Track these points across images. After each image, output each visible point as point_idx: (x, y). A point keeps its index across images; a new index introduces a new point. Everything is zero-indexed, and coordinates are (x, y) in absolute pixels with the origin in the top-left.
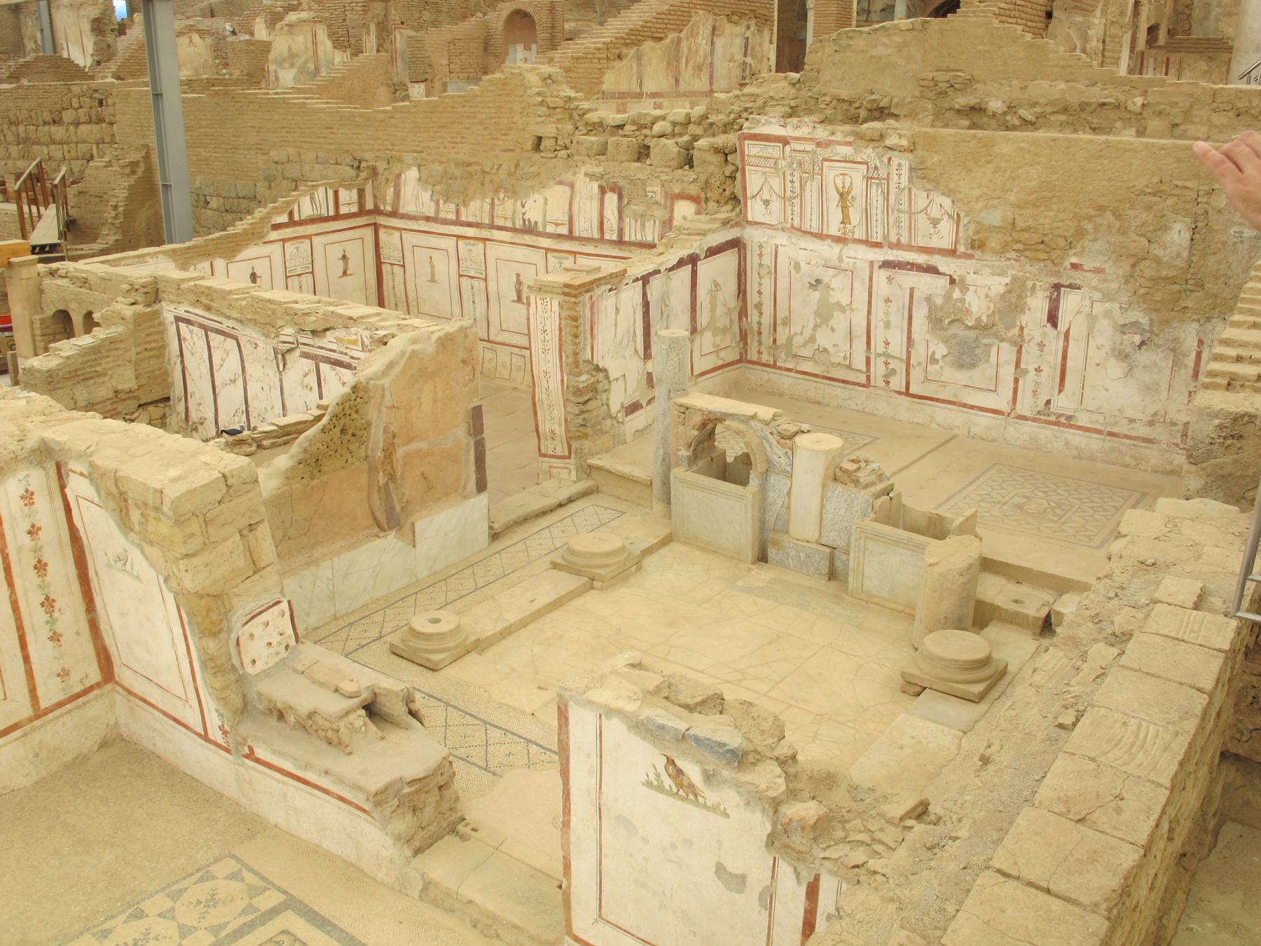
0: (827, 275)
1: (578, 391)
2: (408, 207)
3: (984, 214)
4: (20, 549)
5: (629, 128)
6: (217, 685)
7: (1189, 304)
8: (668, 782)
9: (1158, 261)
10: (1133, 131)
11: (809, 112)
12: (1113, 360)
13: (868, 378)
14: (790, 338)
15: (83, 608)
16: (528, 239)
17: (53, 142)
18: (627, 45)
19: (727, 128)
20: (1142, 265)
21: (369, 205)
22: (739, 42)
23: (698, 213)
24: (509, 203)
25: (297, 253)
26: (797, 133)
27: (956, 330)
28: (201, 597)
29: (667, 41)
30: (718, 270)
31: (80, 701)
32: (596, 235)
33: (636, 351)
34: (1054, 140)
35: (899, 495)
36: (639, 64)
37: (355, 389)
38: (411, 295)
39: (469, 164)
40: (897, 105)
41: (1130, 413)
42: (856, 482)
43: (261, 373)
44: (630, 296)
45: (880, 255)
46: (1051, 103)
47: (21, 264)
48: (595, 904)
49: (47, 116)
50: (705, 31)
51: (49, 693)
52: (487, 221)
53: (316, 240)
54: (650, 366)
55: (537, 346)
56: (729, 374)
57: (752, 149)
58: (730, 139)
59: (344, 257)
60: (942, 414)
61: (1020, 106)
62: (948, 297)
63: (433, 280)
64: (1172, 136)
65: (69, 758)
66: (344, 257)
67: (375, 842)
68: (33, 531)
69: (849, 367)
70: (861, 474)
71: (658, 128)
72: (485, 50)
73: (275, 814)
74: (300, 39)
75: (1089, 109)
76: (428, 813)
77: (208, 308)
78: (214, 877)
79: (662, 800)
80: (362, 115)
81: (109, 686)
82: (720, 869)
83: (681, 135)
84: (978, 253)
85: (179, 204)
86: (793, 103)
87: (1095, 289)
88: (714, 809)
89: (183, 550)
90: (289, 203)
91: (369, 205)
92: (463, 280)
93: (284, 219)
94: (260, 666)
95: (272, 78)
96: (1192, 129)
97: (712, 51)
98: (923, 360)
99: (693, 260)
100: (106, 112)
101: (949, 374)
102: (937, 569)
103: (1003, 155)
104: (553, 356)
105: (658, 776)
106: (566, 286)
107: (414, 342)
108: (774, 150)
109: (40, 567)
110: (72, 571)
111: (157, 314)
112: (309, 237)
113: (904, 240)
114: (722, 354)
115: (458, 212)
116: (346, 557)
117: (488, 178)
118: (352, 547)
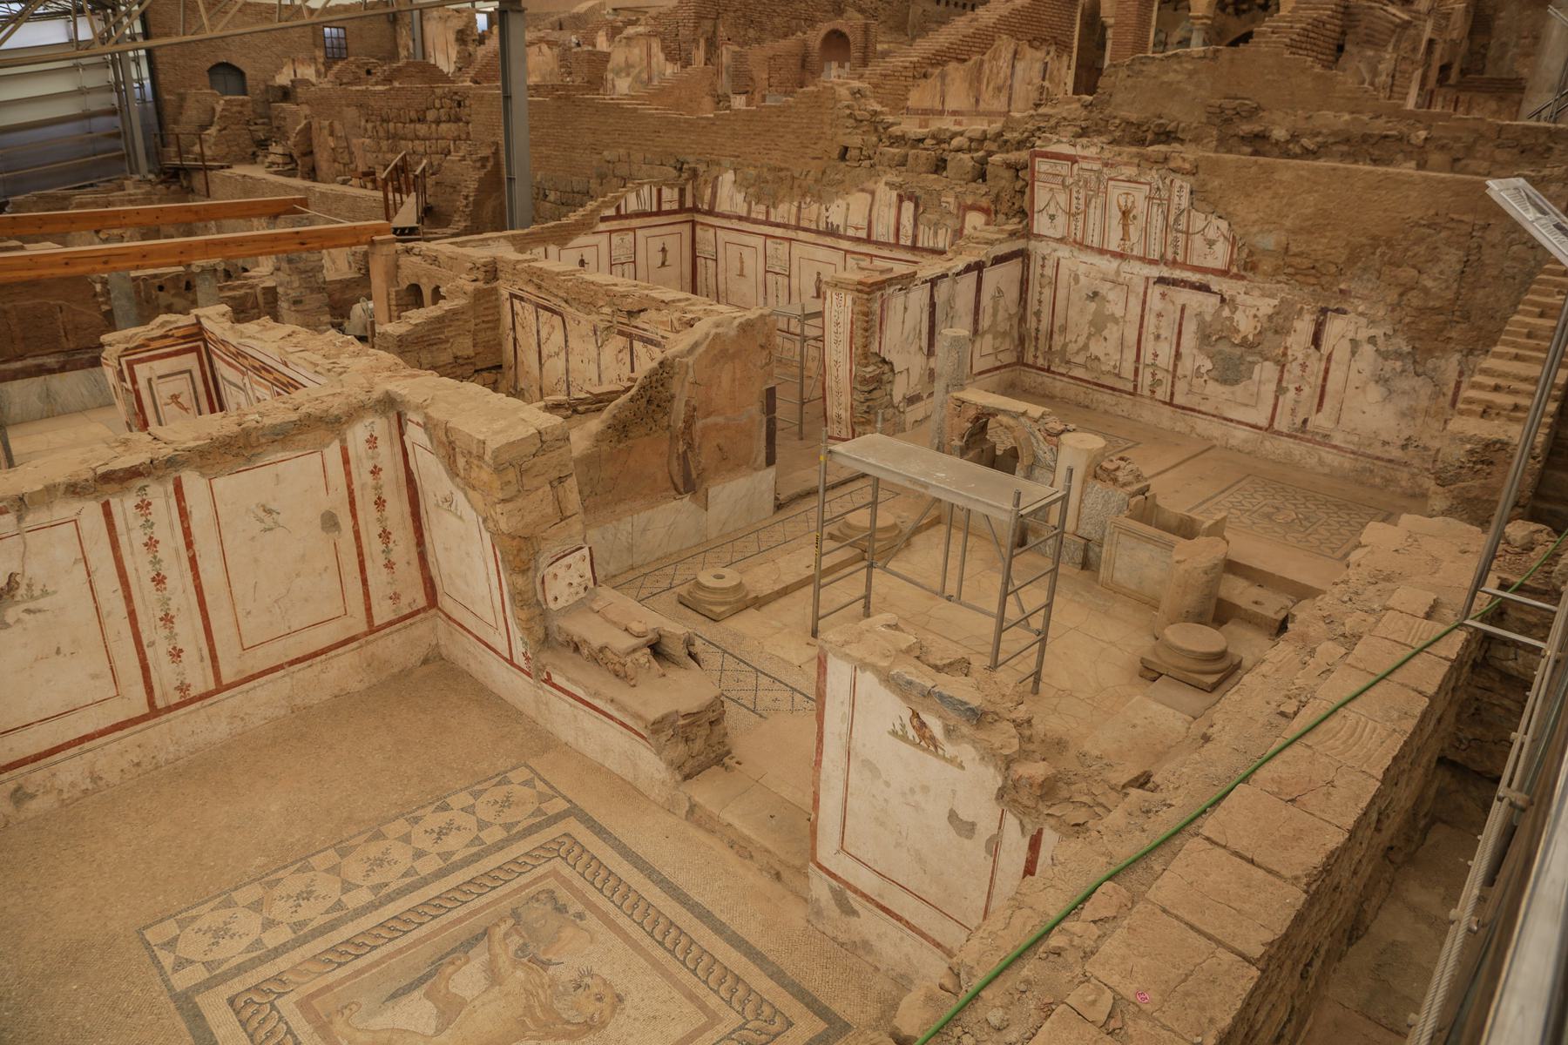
0: (1104, 289)
1: (864, 381)
2: (723, 206)
3: (1258, 238)
4: (363, 486)
5: (929, 142)
6: (523, 616)
7: (1453, 334)
8: (911, 733)
9: (1426, 291)
10: (1413, 164)
11: (1099, 133)
12: (1372, 384)
13: (1135, 387)
14: (1065, 345)
15: (414, 541)
16: (829, 241)
17: (417, 138)
18: (932, 65)
19: (1020, 145)
20: (1410, 295)
21: (689, 204)
22: (1038, 66)
23: (987, 224)
24: (815, 207)
25: (621, 243)
26: (1086, 153)
27: (1224, 347)
28: (514, 538)
29: (971, 63)
30: (1001, 278)
31: (408, 622)
32: (892, 241)
34: (1334, 169)
35: (1154, 496)
36: (943, 84)
37: (661, 364)
38: (722, 287)
39: (781, 170)
40: (1183, 130)
41: (1385, 436)
42: (1115, 480)
43: (583, 348)
44: (919, 296)
45: (1155, 272)
46: (1334, 134)
47: (382, 242)
48: (837, 836)
49: (413, 115)
50: (1007, 55)
51: (383, 612)
52: (793, 222)
53: (639, 232)
54: (932, 363)
55: (830, 337)
56: (1006, 375)
57: (1042, 166)
58: (1023, 155)
59: (663, 250)
60: (1203, 426)
61: (1303, 135)
62: (1217, 313)
63: (741, 275)
64: (1452, 170)
65: (396, 670)
66: (663, 250)
67: (650, 766)
68: (375, 471)
69: (1118, 376)
70: (1119, 473)
71: (955, 142)
72: (803, 66)
73: (565, 733)
74: (636, 51)
75: (1372, 141)
76: (698, 745)
77: (539, 287)
78: (510, 783)
79: (905, 749)
80: (686, 121)
81: (433, 611)
82: (952, 816)
83: (977, 150)
84: (1250, 275)
85: (521, 194)
86: (1083, 124)
87: (1361, 314)
88: (951, 761)
89: (500, 496)
90: (617, 198)
91: (689, 204)
92: (769, 276)
93: (611, 212)
94: (561, 603)
95: (609, 86)
96: (1473, 164)
97: (1012, 74)
98: (1188, 373)
99: (978, 267)
100: (464, 112)
101: (1213, 388)
102: (1182, 567)
103: (1281, 182)
104: (844, 347)
105: (903, 726)
106: (860, 283)
107: (718, 325)
108: (1063, 168)
109: (380, 503)
110: (407, 508)
111: (495, 290)
112: (633, 230)
113: (1180, 259)
115: (768, 213)
116: (645, 515)
117: (797, 183)
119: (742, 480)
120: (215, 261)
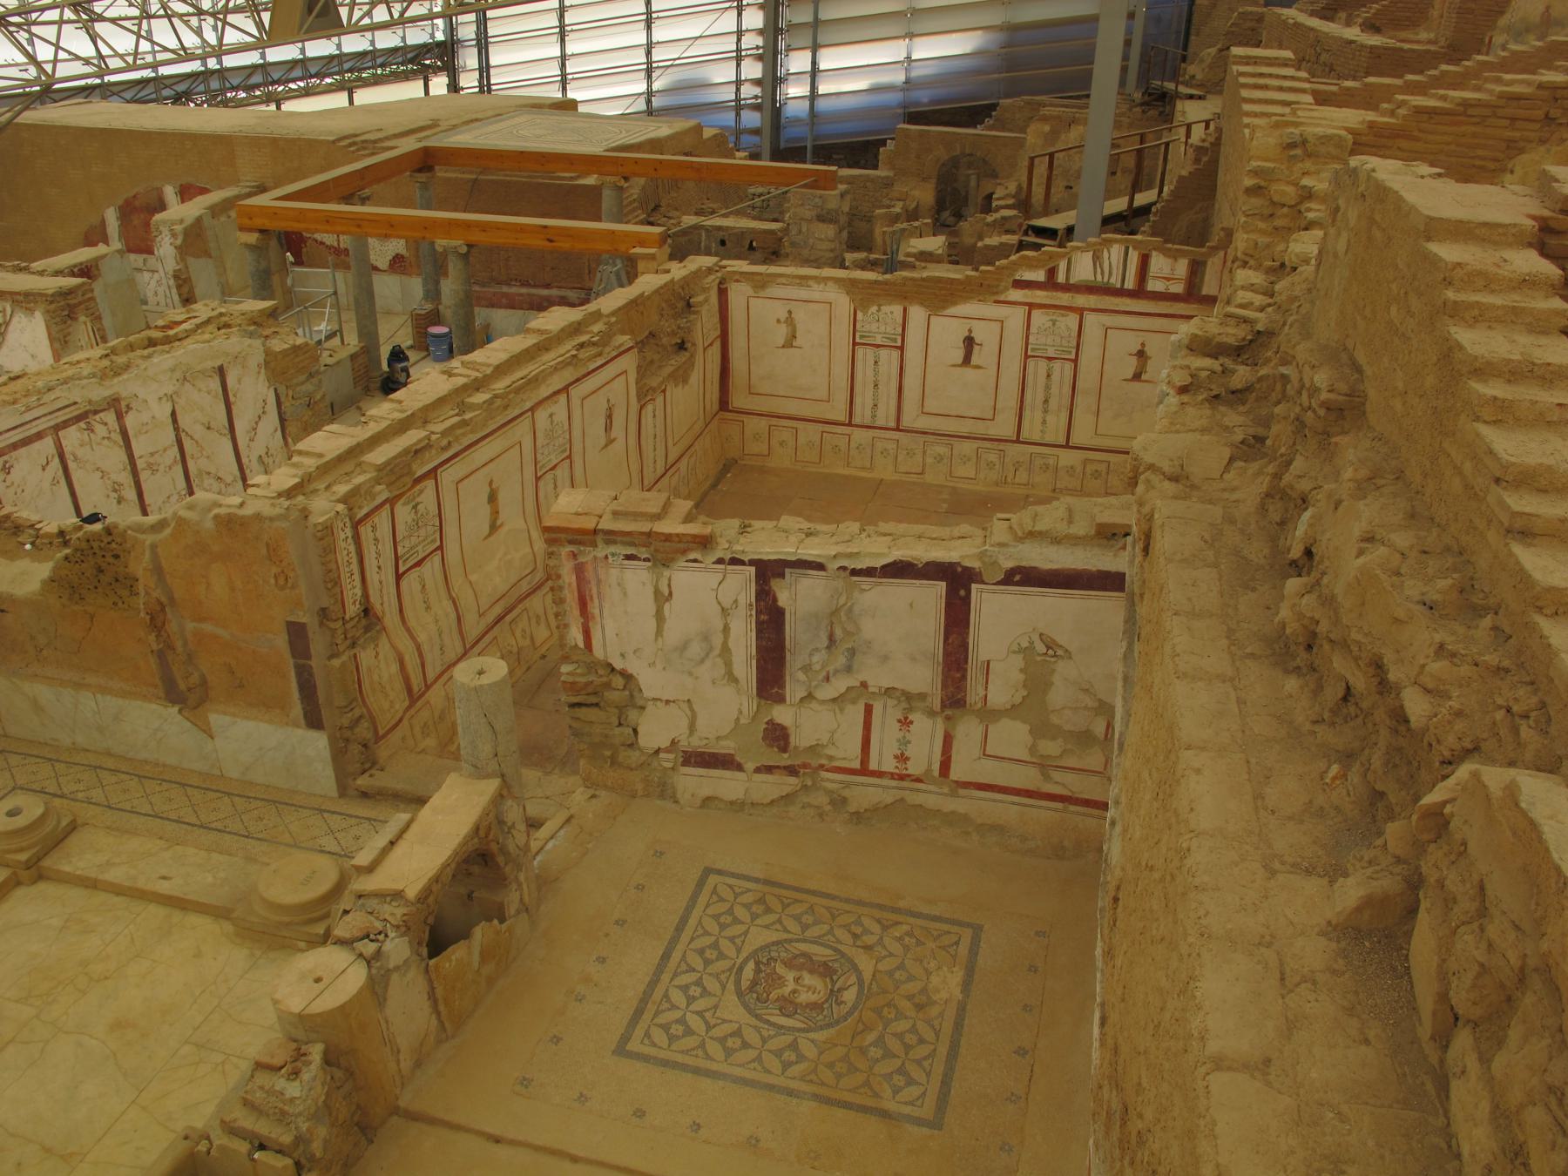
21: (1208, 289)
25: (1052, 330)
33: (733, 679)
59: (1141, 354)
66: (1141, 354)
90: (1051, 256)
93: (1039, 276)
112: (1080, 311)
114: (1057, 776)
116: (111, 703)
118: (125, 695)
120: (458, 243)
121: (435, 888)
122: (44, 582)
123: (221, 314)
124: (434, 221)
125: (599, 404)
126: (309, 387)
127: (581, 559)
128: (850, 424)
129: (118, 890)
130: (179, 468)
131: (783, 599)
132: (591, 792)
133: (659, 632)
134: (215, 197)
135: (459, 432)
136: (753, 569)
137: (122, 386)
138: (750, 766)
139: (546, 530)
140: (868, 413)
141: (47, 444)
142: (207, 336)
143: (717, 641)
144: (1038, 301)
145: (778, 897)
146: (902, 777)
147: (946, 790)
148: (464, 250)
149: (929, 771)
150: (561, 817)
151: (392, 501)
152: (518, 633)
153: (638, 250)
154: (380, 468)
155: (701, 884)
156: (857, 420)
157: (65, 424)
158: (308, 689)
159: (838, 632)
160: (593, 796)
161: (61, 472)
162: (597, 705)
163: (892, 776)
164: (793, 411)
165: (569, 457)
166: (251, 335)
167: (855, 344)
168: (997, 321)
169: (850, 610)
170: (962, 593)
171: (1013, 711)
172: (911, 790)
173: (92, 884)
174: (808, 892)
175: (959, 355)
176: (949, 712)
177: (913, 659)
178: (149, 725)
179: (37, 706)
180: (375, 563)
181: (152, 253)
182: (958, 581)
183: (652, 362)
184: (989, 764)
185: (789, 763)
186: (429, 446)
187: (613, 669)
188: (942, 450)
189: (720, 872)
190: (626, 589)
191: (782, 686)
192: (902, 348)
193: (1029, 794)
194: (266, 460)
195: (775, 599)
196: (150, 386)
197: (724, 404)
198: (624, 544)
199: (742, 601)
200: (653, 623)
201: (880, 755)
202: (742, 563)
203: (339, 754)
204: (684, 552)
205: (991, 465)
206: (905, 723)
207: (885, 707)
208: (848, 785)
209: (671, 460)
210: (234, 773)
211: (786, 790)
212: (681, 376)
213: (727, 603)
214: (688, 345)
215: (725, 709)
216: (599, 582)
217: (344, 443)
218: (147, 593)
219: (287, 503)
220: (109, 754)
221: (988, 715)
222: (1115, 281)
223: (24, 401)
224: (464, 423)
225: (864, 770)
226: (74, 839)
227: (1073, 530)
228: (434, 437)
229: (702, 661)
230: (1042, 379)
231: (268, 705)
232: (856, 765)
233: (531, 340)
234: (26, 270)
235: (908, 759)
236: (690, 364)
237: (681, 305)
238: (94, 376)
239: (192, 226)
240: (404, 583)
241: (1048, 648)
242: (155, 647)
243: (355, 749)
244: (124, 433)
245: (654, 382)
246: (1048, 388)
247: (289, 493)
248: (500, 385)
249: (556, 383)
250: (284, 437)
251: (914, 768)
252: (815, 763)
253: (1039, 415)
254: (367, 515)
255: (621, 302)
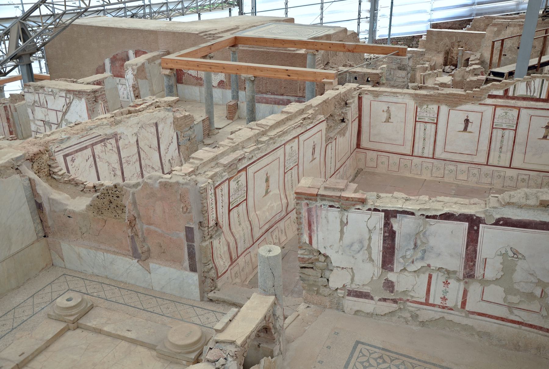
25: (506, 116)
33: (371, 260)
90: (506, 84)
93: (501, 93)
112: (519, 108)
114: (516, 312)
116: (110, 256)
119: (172, 270)
120: (251, 76)
121: (248, 341)
122: (87, 206)
123: (157, 102)
124: (241, 66)
125: (310, 143)
126: (190, 132)
127: (310, 206)
128: (412, 156)
129: (109, 334)
130: (138, 163)
131: (395, 227)
132: (307, 305)
133: (341, 238)
134: (149, 55)
135: (256, 152)
136: (383, 214)
137: (119, 129)
138: (376, 298)
139: (296, 193)
140: (420, 151)
141: (89, 151)
142: (151, 110)
143: (366, 243)
144: (499, 104)
145: (389, 356)
146: (444, 308)
147: (464, 315)
148: (253, 79)
149: (456, 305)
150: (295, 314)
151: (229, 179)
152: (274, 237)
153: (325, 80)
154: (225, 166)
155: (355, 348)
156: (415, 154)
157: (96, 143)
158: (192, 255)
159: (418, 242)
160: (308, 307)
161: (93, 163)
162: (312, 268)
163: (439, 306)
164: (388, 150)
165: (298, 165)
166: (169, 110)
167: (416, 121)
168: (480, 113)
169: (425, 233)
170: (475, 228)
171: (496, 281)
172: (448, 313)
173: (98, 331)
174: (401, 355)
175: (462, 127)
176: (466, 280)
177: (451, 256)
178: (125, 266)
179: (79, 257)
180: (221, 204)
181: (122, 76)
182: (474, 222)
183: (331, 127)
184: (484, 304)
185: (394, 297)
186: (244, 158)
187: (320, 253)
188: (452, 168)
189: (363, 343)
190: (329, 219)
191: (393, 264)
192: (436, 124)
193: (503, 319)
194: (171, 161)
195: (392, 227)
196: (128, 130)
197: (358, 146)
198: (328, 200)
199: (378, 227)
200: (339, 235)
201: (434, 297)
202: (379, 211)
203: (202, 282)
204: (354, 205)
205: (474, 175)
206: (446, 283)
207: (438, 276)
208: (419, 309)
209: (337, 168)
210: (158, 289)
211: (393, 309)
212: (342, 133)
213: (371, 228)
214: (345, 120)
215: (368, 272)
216: (317, 216)
217: (212, 155)
218: (129, 212)
219: (189, 178)
220: (107, 278)
221: (484, 282)
222: (536, 95)
223: (82, 133)
224: (259, 149)
225: (427, 303)
226: (92, 312)
227: (529, 202)
228: (246, 154)
229: (359, 252)
230: (499, 138)
231: (175, 261)
232: (423, 300)
233: (284, 116)
234: (76, 82)
235: (446, 299)
236: (346, 128)
237: (343, 103)
238: (108, 124)
239: (140, 67)
240: (231, 213)
241: (514, 254)
242: (130, 235)
243: (209, 281)
244: (118, 148)
245: (332, 135)
246: (502, 141)
247: (190, 174)
248: (272, 133)
249: (294, 133)
250: (179, 152)
251: (449, 304)
252: (405, 298)
253: (497, 153)
254: (219, 185)
255: (320, 102)
